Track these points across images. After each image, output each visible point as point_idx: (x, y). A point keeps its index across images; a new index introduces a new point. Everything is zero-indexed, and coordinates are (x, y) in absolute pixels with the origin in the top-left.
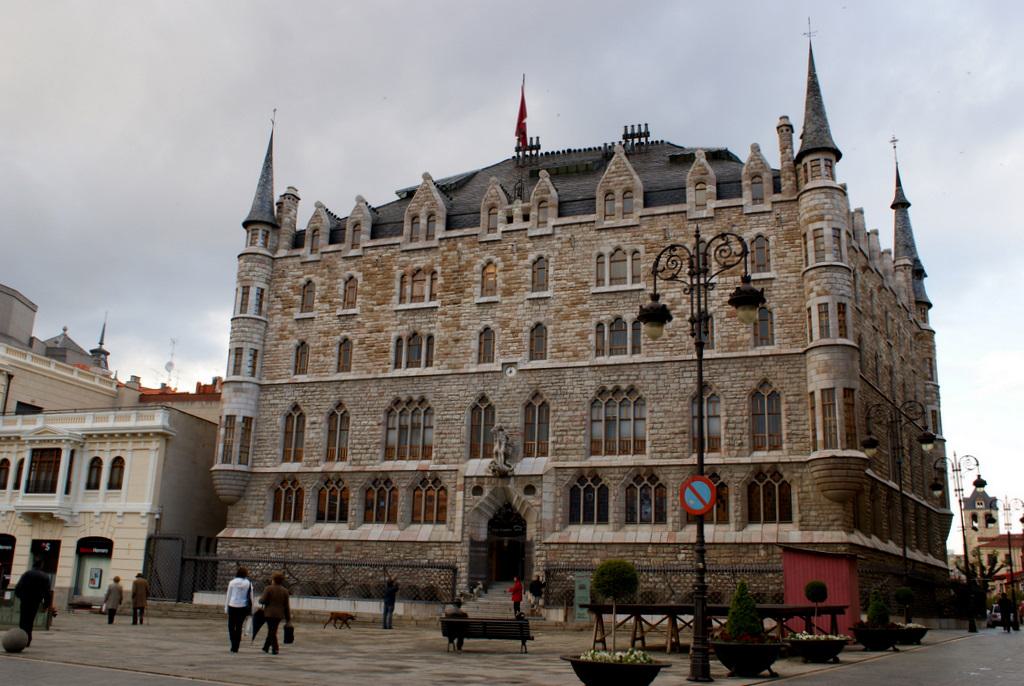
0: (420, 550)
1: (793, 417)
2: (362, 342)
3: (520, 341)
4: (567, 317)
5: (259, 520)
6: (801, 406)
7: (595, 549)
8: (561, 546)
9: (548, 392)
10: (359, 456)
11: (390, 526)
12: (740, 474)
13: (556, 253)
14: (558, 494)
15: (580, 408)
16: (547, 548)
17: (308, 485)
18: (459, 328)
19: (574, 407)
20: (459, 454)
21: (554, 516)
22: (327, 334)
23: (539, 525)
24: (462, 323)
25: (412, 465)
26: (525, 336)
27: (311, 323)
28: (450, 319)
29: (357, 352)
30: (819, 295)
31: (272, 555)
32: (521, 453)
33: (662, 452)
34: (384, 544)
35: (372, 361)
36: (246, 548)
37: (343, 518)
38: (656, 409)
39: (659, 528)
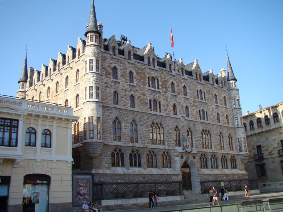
0: (169, 177)
1: (236, 143)
2: (138, 98)
3: (183, 110)
4: (193, 106)
5: (108, 166)
6: (236, 141)
7: (209, 176)
9: (192, 128)
10: (144, 142)
11: (156, 169)
12: (230, 157)
13: (188, 86)
16: (200, 176)
17: (128, 152)
18: (168, 101)
22: (125, 90)
24: (168, 100)
25: (161, 147)
26: (184, 109)
27: (118, 84)
28: (165, 97)
29: (136, 101)
30: (240, 115)
31: (119, 181)
33: (216, 149)
34: (159, 176)
35: (143, 106)
36: (107, 178)
37: (140, 166)
38: (214, 137)
39: (218, 170)
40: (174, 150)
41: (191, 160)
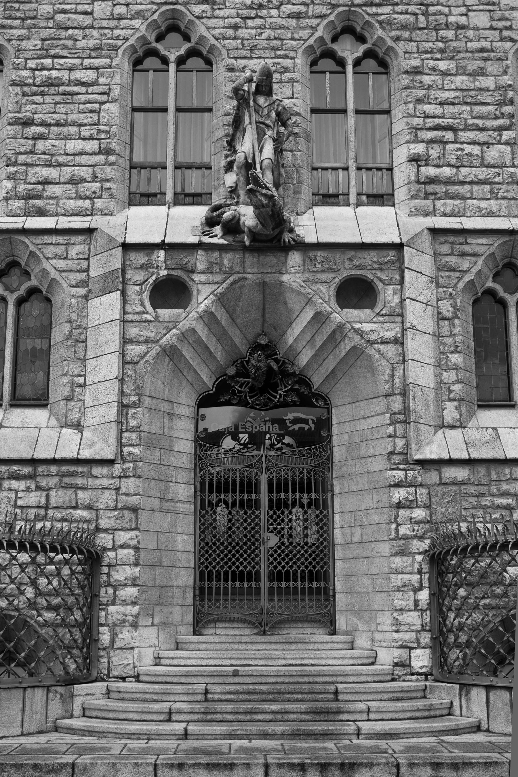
8: (482, 470)
14: (446, 308)
15: (492, 67)
16: (433, 477)
19: (472, 66)
20: (95, 186)
21: (438, 376)
23: (397, 404)
32: (306, 194)
40: (90, 231)
41: (309, 314)
